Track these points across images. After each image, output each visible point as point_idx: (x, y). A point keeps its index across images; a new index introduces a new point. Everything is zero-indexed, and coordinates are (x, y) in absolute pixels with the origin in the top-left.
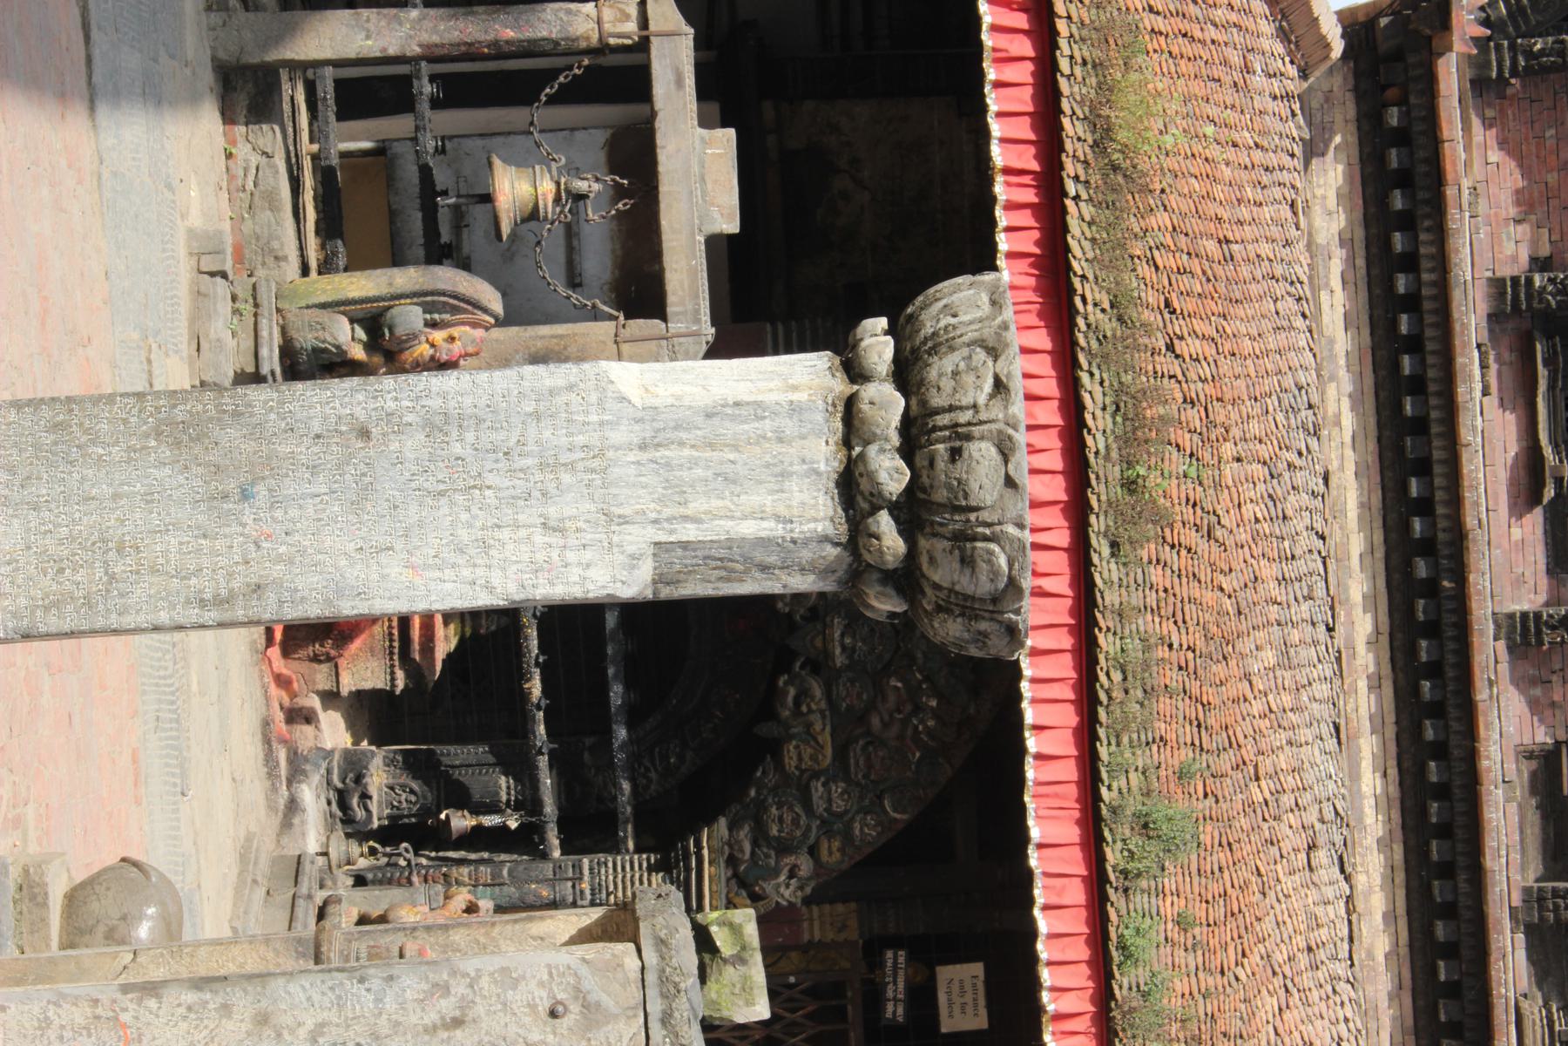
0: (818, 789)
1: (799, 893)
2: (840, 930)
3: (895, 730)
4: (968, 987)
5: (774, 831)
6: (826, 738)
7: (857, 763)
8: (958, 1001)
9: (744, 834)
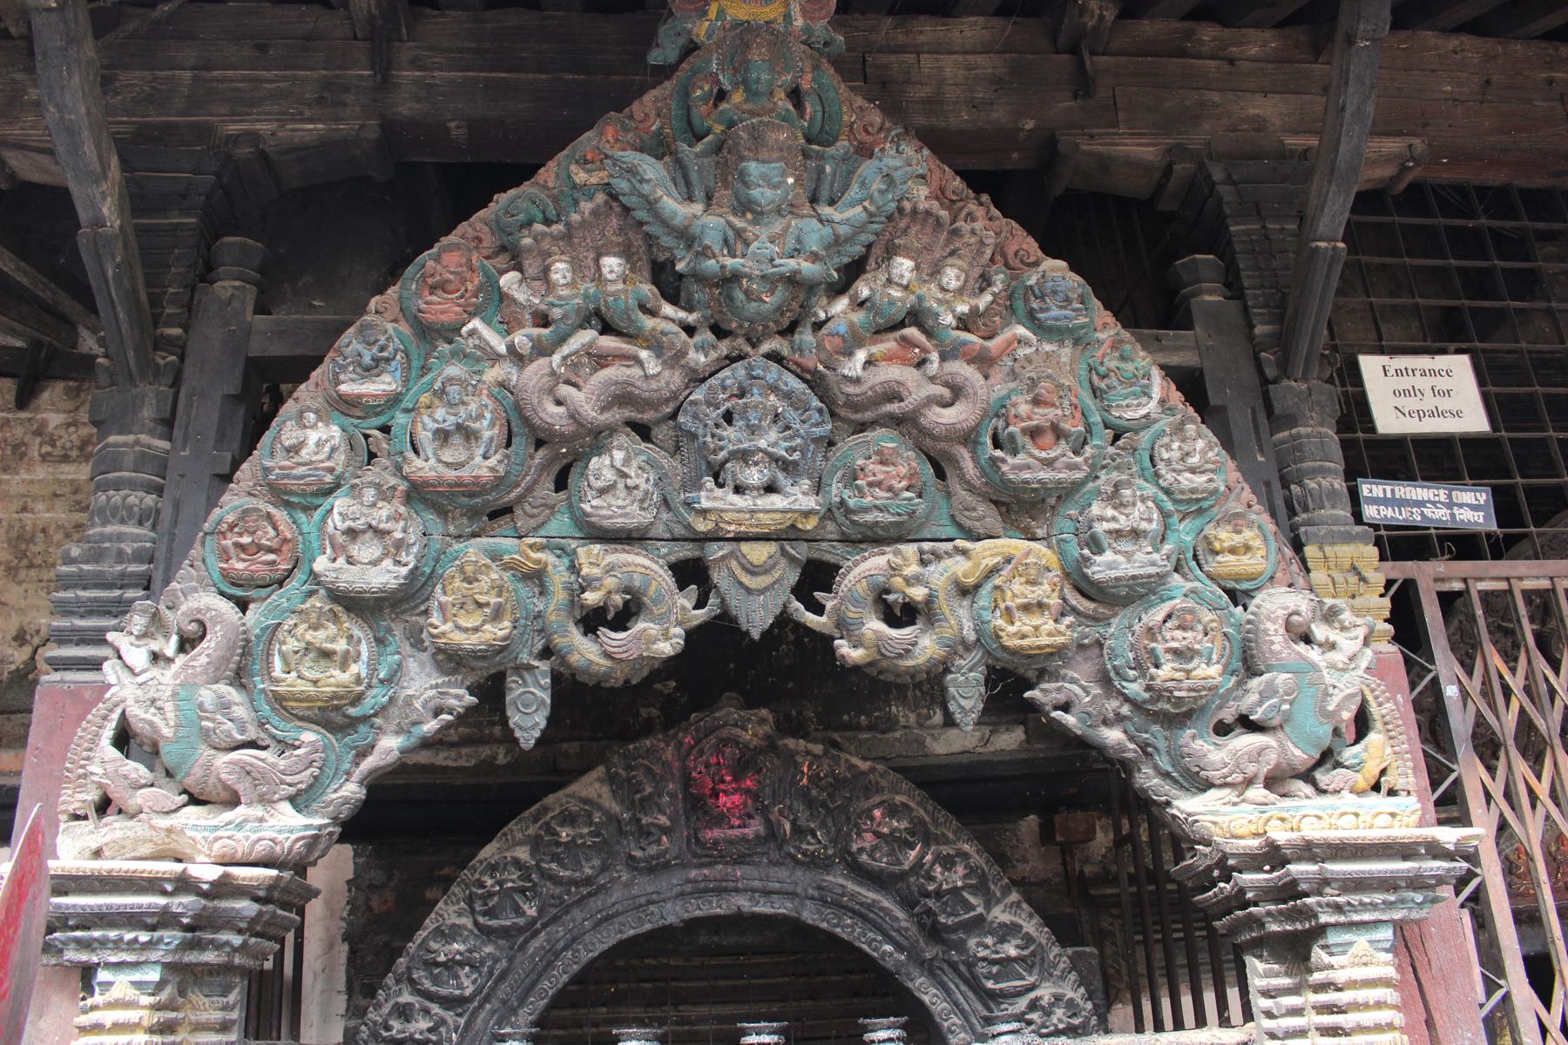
0: (1108, 565)
1: (1347, 616)
2: (1363, 579)
3: (963, 370)
4: (1405, 383)
5: (1209, 671)
6: (987, 552)
7: (1049, 463)
8: (1429, 403)
9: (1216, 754)
